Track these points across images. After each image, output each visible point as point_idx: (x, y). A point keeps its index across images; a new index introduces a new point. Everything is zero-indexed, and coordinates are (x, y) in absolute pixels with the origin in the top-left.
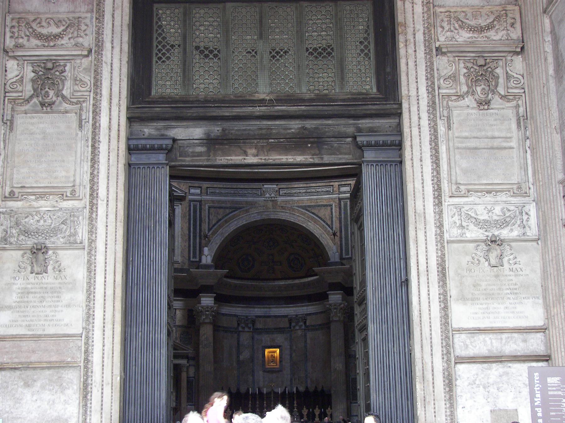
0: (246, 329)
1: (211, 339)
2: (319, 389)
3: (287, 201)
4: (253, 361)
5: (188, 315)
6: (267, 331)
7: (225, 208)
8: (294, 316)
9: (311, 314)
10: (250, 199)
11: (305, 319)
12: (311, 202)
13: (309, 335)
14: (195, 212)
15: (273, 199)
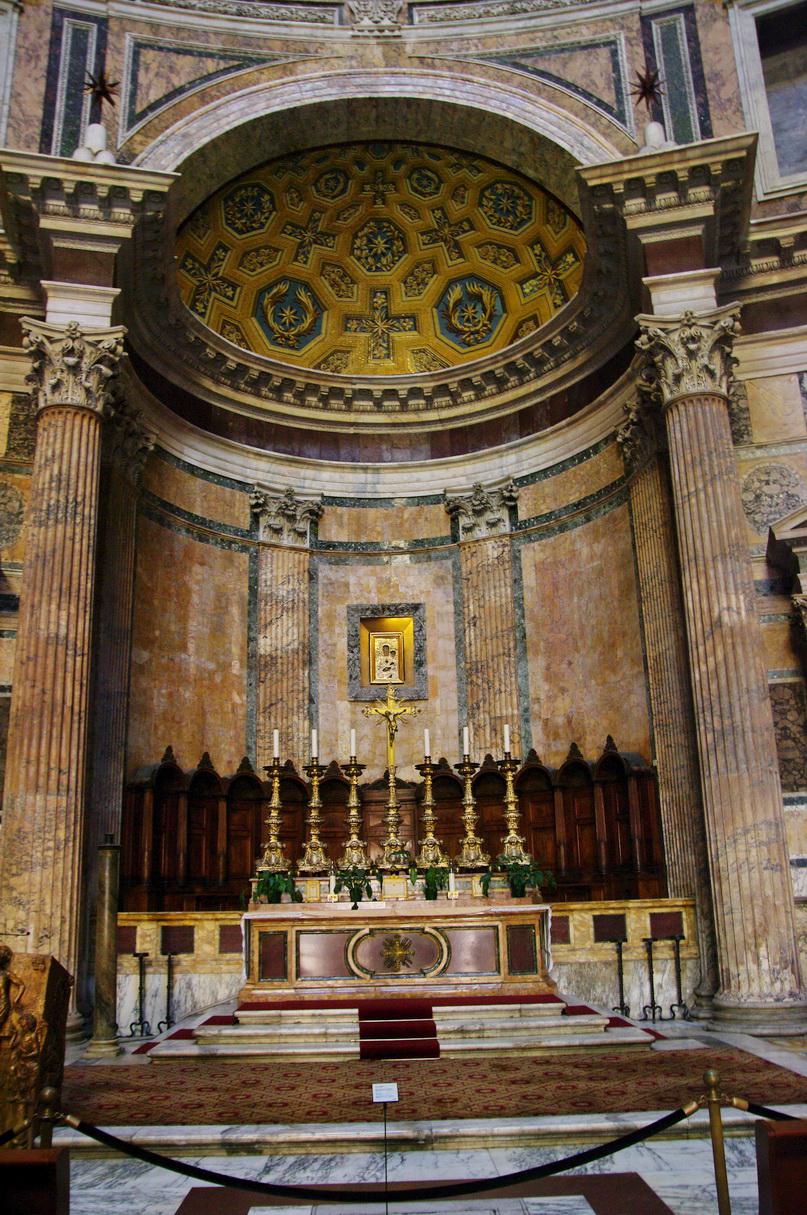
0: (287, 540)
1: (87, 488)
2: (592, 754)
3: (439, 42)
4: (310, 661)
5: (14, 418)
6: (369, 552)
7: (200, 54)
8: (471, 493)
9: (533, 475)
10: (300, 31)
11: (511, 499)
12: (532, 40)
13: (532, 554)
14: (79, 51)
15: (387, 33)
